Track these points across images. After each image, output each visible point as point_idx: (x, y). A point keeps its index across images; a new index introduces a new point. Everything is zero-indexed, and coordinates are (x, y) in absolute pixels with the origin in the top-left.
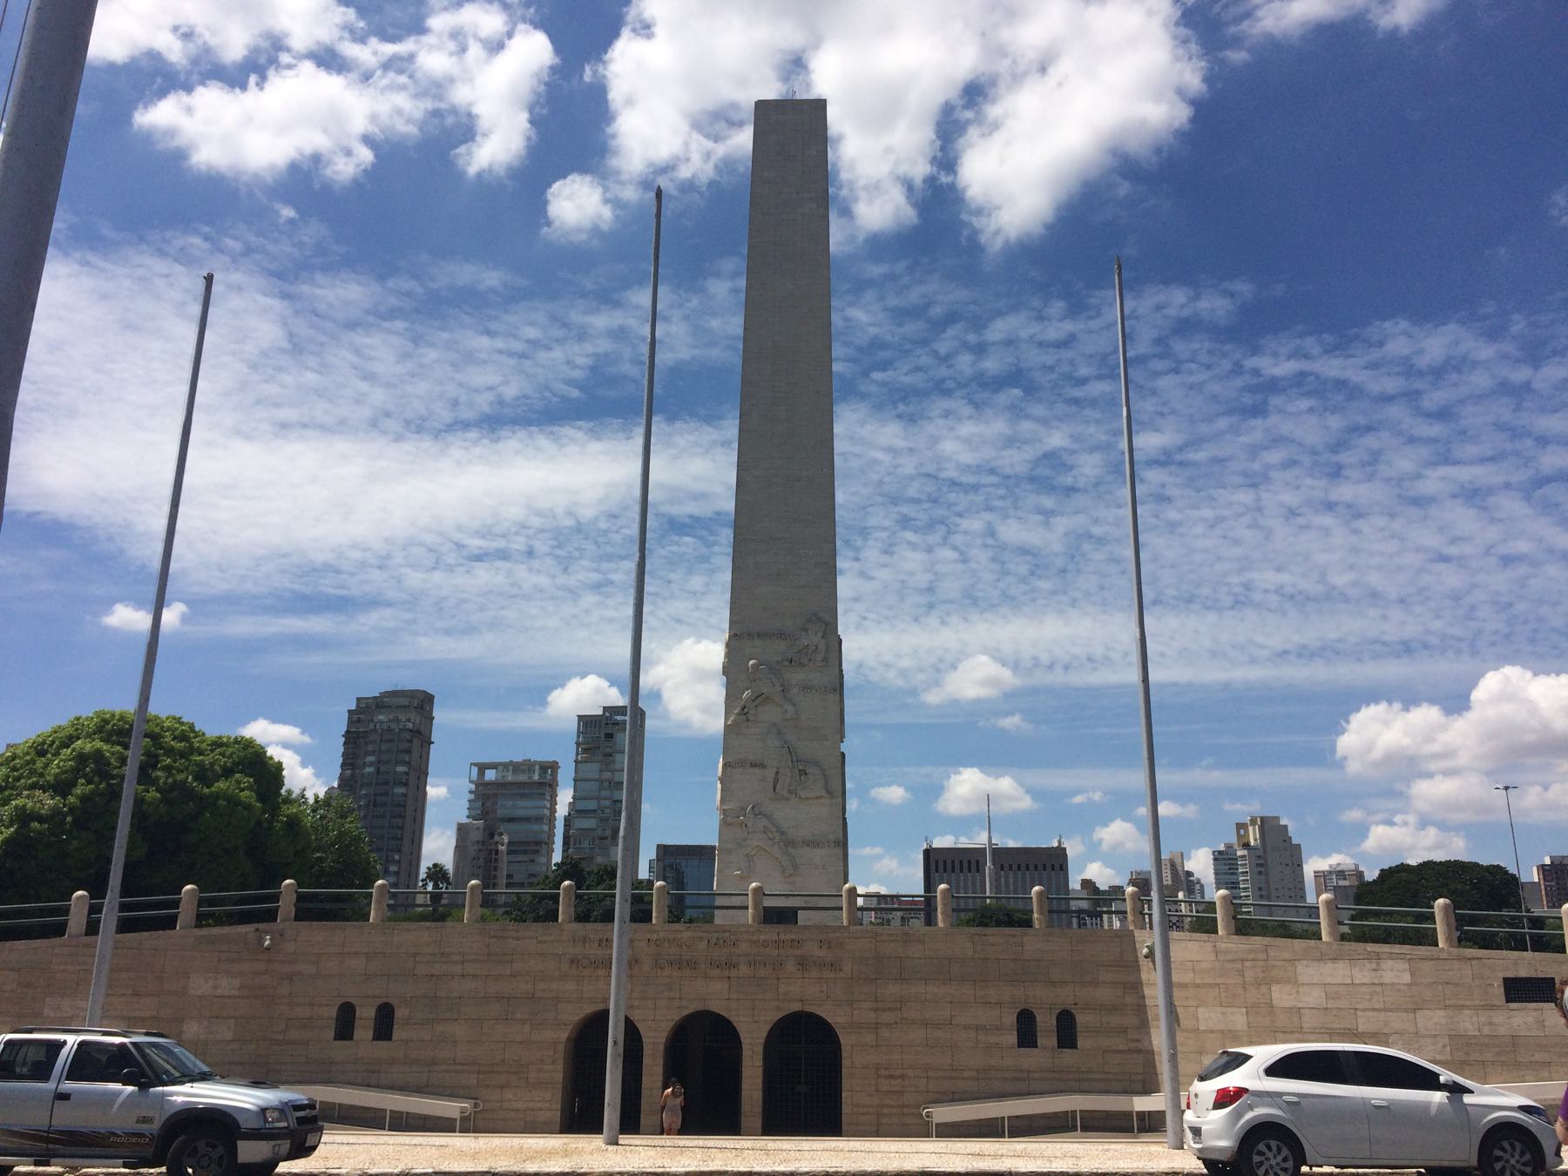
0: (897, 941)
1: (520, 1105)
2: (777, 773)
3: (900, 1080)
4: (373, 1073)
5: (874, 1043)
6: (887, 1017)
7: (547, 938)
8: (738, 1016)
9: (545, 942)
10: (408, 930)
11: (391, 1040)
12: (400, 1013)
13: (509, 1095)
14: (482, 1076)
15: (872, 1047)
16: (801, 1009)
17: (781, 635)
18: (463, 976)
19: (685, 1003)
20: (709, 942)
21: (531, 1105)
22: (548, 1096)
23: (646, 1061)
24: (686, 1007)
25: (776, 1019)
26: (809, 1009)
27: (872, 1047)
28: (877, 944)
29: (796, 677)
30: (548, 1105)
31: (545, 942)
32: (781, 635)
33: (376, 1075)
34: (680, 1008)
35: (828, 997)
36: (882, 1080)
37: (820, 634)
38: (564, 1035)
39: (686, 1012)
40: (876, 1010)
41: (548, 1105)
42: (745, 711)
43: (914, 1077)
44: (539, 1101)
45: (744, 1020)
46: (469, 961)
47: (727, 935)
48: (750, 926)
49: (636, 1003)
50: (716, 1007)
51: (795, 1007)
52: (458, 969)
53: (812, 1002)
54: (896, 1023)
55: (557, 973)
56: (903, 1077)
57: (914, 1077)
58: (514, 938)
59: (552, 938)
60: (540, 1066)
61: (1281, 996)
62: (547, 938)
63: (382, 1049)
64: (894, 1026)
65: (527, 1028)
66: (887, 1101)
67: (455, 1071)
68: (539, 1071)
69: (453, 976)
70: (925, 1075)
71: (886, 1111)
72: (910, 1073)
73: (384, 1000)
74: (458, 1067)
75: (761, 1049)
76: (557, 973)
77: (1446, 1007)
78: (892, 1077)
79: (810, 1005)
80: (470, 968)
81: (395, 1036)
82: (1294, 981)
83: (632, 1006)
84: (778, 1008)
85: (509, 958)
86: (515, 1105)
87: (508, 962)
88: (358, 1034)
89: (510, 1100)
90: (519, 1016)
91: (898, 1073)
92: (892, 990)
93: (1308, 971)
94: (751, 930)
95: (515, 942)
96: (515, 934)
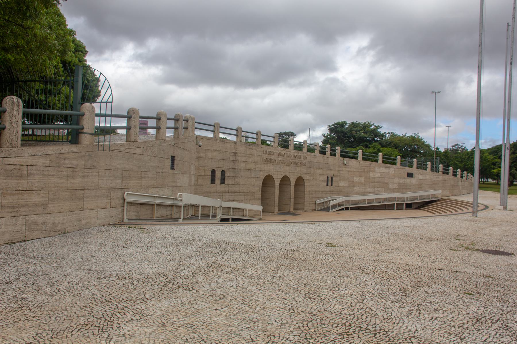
61: (372, 175)
63: (222, 188)
68: (257, 194)
74: (240, 194)
77: (399, 178)
82: (374, 171)
85: (250, 156)
93: (377, 170)
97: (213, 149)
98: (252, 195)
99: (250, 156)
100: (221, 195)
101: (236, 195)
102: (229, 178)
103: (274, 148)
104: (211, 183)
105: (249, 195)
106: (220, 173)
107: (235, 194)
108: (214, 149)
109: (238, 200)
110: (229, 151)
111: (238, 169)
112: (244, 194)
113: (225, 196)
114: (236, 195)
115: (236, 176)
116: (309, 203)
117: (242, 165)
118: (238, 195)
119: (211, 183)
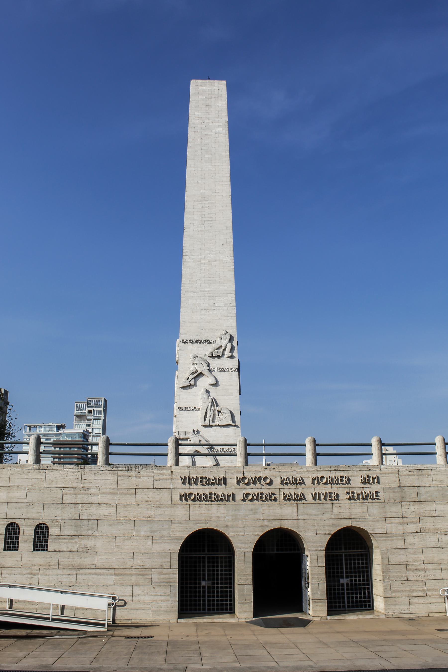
0: (414, 475)
1: (147, 599)
2: (206, 412)
3: (423, 572)
4: (34, 575)
5: (403, 547)
6: (411, 528)
7: (161, 477)
8: (305, 531)
9: (160, 480)
10: (56, 470)
11: (47, 550)
12: (53, 531)
13: (137, 590)
14: (116, 577)
15: (401, 549)
16: (350, 525)
17: (208, 342)
18: (99, 504)
19: (266, 523)
20: (281, 478)
21: (155, 598)
22: (168, 591)
23: (237, 564)
24: (267, 526)
25: (332, 533)
26: (355, 524)
27: (401, 549)
28: (400, 477)
29: (215, 363)
30: (168, 598)
31: (160, 480)
32: (208, 342)
33: (37, 577)
34: (261, 526)
35: (369, 515)
36: (411, 572)
37: (228, 340)
38: (177, 547)
39: (267, 529)
40: (403, 524)
41: (168, 598)
42: (189, 380)
43: (433, 569)
44: (161, 595)
45: (309, 534)
46: (104, 493)
47: (294, 473)
48: (310, 467)
49: (229, 523)
50: (287, 525)
51: (346, 524)
52: (95, 499)
53: (358, 520)
54: (417, 532)
55: (170, 503)
56: (424, 570)
57: (433, 569)
58: (136, 477)
59: (165, 477)
60: (160, 570)
62: (161, 477)
64: (416, 534)
65: (149, 543)
66: (414, 588)
67: (96, 574)
68: (160, 573)
69: (92, 504)
70: (439, 567)
71: (414, 594)
72: (429, 566)
73: (41, 521)
74: (98, 571)
75: (324, 553)
76: (170, 503)
78: (417, 570)
79: (356, 521)
80: (104, 499)
81: (50, 547)
83: (227, 526)
84: (333, 525)
85: (133, 491)
86: (143, 598)
87: (132, 494)
88: (21, 546)
89: (138, 595)
90: (142, 533)
91: (420, 567)
92: (413, 509)
94: (311, 469)
95: (138, 480)
96: (137, 474)
97: (11, 485)
98: (143, 575)
99: (133, 491)
100: (35, 571)
101: (82, 574)
102: (60, 539)
103: (220, 469)
104: (5, 550)
105: (131, 575)
106: (34, 529)
107: (81, 571)
108: (16, 484)
109: (90, 583)
110: (61, 485)
111: (89, 520)
112: (112, 571)
113: (45, 575)
114: (82, 574)
115: (84, 533)
116: (407, 594)
117: (104, 511)
118: (90, 574)
119: (5, 550)
